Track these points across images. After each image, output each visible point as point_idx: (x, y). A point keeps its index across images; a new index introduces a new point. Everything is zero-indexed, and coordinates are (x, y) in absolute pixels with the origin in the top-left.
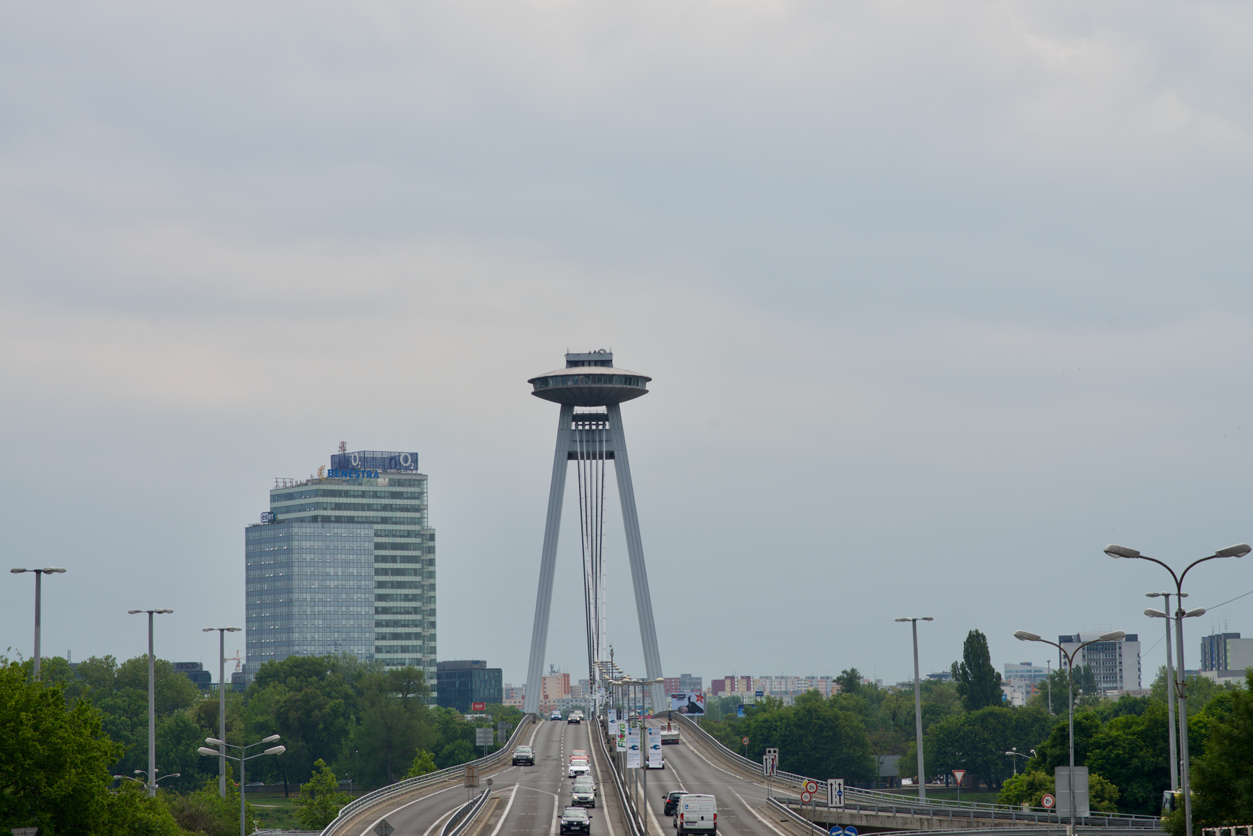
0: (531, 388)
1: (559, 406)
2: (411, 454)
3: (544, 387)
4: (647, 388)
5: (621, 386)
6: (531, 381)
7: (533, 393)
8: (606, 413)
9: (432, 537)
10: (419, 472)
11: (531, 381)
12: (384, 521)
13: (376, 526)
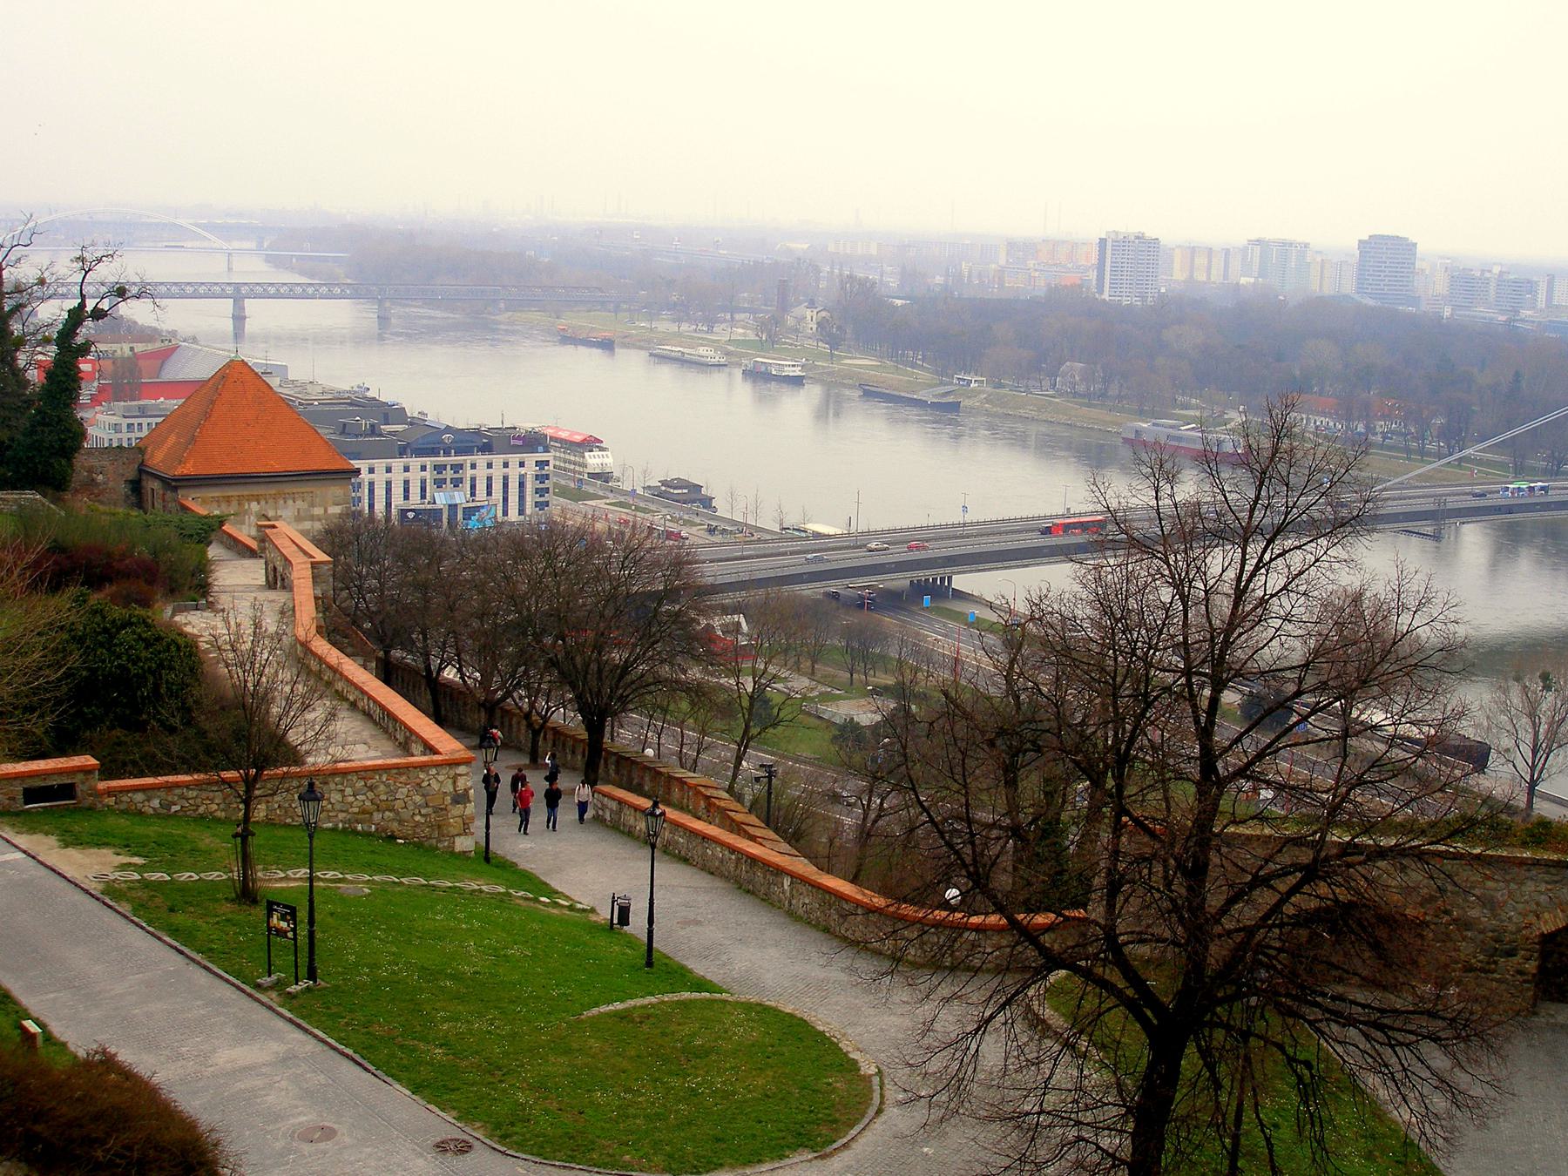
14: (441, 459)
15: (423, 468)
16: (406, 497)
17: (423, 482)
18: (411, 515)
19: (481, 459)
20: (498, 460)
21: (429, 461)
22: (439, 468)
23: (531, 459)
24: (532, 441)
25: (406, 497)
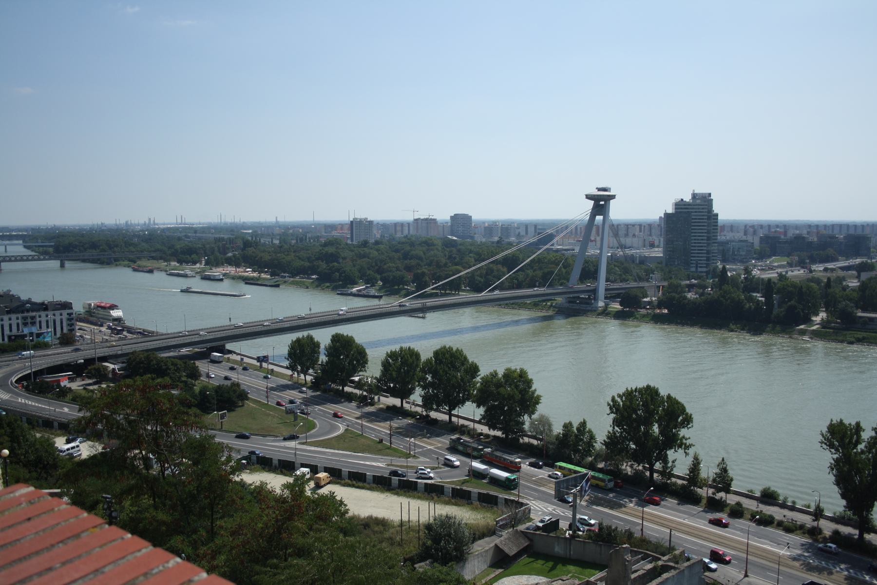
1: (593, 202)
3: (589, 197)
12: (696, 212)
13: (693, 214)
14: (26, 314)
15: (18, 319)
16: (11, 330)
17: (18, 325)
18: (13, 338)
19: (43, 314)
20: (50, 313)
21: (20, 315)
22: (25, 318)
23: (65, 313)
24: (66, 306)
25: (11, 330)
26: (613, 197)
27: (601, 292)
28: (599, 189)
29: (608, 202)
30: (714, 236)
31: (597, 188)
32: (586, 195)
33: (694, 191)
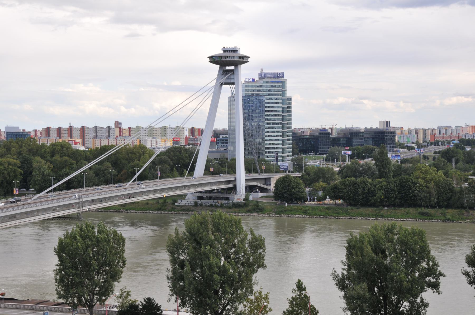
0: (208, 60)
1: (219, 66)
2: (282, 73)
3: (214, 60)
4: (249, 61)
5: (237, 60)
6: (209, 57)
7: (209, 62)
8: (234, 69)
9: (290, 99)
10: (284, 78)
11: (209, 57)
12: (269, 95)
13: (266, 97)
26: (244, 59)
27: (242, 184)
28: (225, 51)
29: (239, 66)
30: (288, 124)
31: (222, 49)
32: (210, 58)
33: (262, 70)
